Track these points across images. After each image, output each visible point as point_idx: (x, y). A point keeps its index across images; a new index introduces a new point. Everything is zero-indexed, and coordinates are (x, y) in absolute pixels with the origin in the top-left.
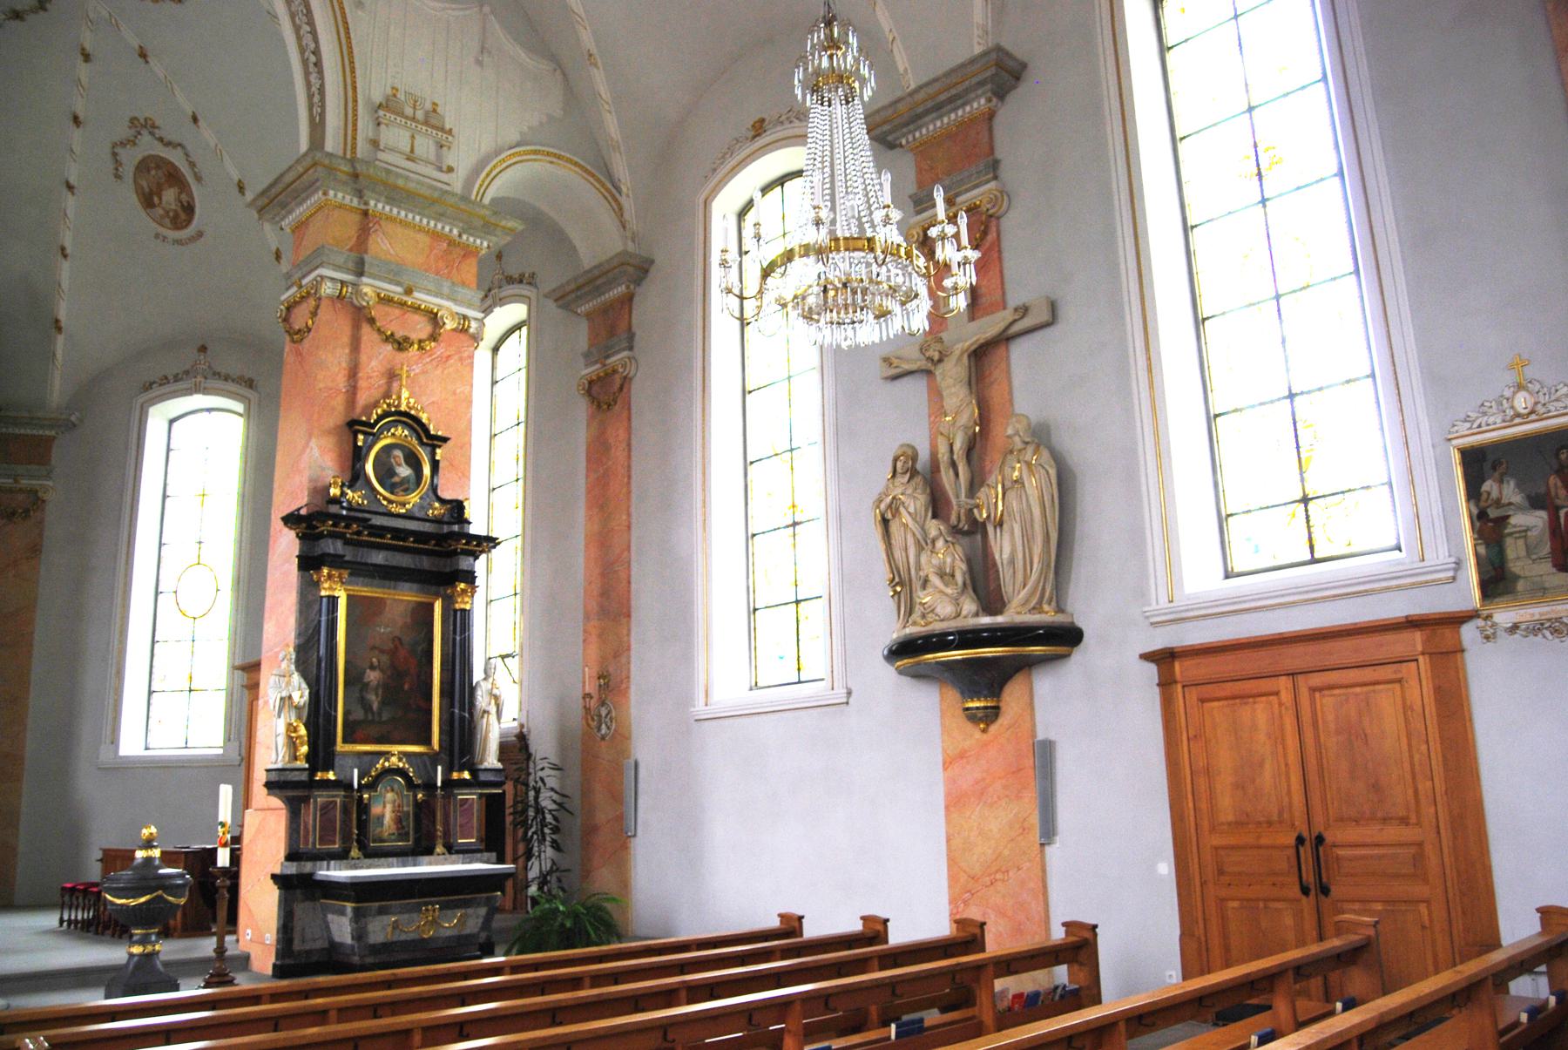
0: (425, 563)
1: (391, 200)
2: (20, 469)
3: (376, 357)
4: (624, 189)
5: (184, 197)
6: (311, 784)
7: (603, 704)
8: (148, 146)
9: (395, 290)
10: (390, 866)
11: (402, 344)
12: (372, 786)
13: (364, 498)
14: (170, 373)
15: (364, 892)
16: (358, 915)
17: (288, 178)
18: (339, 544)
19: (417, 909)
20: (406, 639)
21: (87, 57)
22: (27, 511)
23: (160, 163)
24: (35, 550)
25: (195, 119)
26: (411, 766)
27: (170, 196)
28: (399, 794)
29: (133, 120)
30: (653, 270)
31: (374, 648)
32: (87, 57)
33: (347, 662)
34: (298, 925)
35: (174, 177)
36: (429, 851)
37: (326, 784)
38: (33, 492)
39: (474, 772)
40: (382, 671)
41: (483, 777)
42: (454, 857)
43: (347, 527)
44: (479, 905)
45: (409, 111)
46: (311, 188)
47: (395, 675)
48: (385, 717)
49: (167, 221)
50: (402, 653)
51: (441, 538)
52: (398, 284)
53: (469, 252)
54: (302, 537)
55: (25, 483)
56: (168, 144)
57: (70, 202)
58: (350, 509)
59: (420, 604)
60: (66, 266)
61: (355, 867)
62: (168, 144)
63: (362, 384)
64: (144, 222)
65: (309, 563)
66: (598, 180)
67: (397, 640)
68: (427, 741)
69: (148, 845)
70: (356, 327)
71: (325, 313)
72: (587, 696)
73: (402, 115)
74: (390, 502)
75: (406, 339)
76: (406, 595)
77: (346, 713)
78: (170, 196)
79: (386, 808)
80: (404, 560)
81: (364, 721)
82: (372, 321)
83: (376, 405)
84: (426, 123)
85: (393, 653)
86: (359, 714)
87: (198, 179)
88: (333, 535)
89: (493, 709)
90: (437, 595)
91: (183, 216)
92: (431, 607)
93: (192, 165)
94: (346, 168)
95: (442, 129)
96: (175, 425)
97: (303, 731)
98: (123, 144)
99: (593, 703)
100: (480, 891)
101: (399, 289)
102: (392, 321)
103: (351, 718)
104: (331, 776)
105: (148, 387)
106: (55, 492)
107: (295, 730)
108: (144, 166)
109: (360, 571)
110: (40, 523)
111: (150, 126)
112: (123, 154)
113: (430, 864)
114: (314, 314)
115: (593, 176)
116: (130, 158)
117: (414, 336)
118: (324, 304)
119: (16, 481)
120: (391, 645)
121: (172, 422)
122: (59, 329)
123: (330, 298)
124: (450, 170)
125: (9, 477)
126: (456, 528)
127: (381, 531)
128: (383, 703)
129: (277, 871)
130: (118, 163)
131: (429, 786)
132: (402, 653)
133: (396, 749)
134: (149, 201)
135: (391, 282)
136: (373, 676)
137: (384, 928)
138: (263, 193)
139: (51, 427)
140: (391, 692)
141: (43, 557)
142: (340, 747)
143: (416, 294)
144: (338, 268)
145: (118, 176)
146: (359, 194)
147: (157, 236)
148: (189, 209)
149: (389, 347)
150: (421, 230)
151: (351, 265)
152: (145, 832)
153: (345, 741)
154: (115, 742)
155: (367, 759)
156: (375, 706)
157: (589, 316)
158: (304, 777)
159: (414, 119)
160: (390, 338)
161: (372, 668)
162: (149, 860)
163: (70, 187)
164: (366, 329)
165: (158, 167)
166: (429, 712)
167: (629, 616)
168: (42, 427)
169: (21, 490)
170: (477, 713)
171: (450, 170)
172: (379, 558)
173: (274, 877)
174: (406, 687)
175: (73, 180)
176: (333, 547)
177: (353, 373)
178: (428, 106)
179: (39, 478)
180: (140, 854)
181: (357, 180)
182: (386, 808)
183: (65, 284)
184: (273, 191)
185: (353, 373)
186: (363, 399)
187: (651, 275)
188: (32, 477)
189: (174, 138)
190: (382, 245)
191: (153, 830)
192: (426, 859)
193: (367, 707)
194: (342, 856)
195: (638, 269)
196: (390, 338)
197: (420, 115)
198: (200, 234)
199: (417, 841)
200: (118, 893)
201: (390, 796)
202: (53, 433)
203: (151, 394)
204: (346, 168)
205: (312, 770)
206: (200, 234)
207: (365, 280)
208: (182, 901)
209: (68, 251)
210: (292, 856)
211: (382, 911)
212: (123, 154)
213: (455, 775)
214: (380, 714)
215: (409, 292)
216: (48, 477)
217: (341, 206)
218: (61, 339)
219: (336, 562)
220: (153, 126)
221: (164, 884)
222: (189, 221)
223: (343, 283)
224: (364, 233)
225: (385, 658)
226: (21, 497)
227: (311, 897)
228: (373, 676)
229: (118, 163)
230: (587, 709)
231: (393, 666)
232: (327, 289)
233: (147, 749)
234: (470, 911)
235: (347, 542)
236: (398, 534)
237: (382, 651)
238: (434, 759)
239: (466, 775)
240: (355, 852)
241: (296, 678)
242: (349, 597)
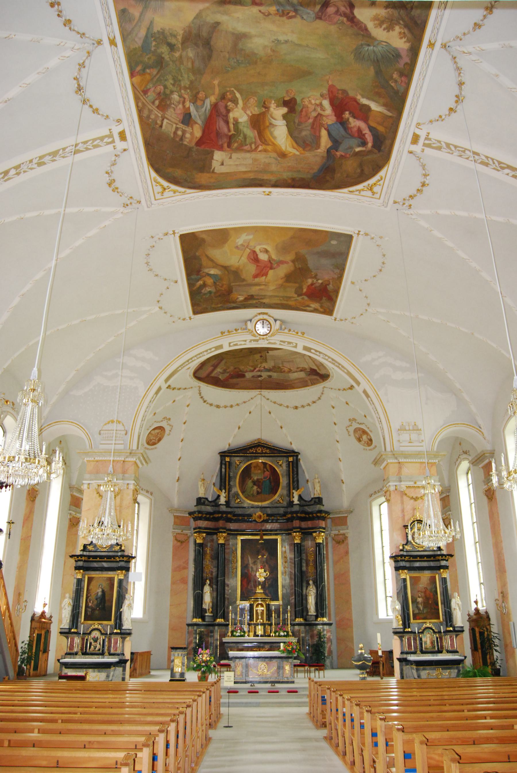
0: (432, 564)
1: (405, 458)
2: (339, 527)
3: (409, 504)
4: (482, 427)
5: (369, 437)
6: (404, 632)
7: (503, 602)
8: (355, 425)
9: (411, 484)
10: (429, 656)
11: (416, 499)
12: (422, 633)
13: (410, 547)
14: (377, 490)
15: (419, 664)
16: (417, 670)
17: (378, 458)
18: (404, 562)
19: (434, 669)
20: (429, 588)
21: (333, 407)
22: (343, 541)
23: (360, 429)
24: (347, 553)
25: (365, 416)
26: (434, 626)
27: (365, 437)
28: (431, 635)
29: (350, 420)
30: (495, 452)
31: (418, 591)
32: (333, 407)
33: (412, 597)
34: (405, 673)
35: (364, 432)
36: (441, 652)
37: (408, 632)
38: (344, 534)
39: (454, 627)
40: (423, 598)
41: (456, 629)
42: (449, 654)
43: (405, 558)
44: (454, 669)
45: (407, 428)
46: (384, 460)
47: (426, 599)
48: (425, 612)
49: (366, 445)
50: (428, 592)
51: (434, 556)
52: (412, 481)
53: (433, 464)
54: (395, 561)
55: (342, 532)
56: (361, 424)
57: (338, 445)
58: (407, 551)
59: (431, 577)
60: (341, 464)
61: (418, 656)
62: (361, 424)
63: (406, 514)
64: (359, 446)
65: (397, 569)
66: (473, 427)
67: (426, 588)
68: (439, 618)
69: (361, 649)
70: (402, 497)
71: (392, 496)
72: (496, 600)
73: (406, 430)
74: (418, 547)
75: (416, 497)
76: (426, 575)
77: (413, 611)
78: (365, 437)
79: (427, 639)
80: (425, 564)
81: (417, 614)
82: (406, 494)
83: (410, 519)
84: (413, 430)
85: (425, 592)
86: (417, 611)
87: (371, 431)
88: (401, 561)
89: (458, 608)
90: (437, 573)
91: (370, 442)
92: (435, 577)
93: (368, 428)
94: (390, 453)
95: (418, 430)
96: (381, 506)
97: (400, 617)
98: (348, 427)
99: (500, 602)
100: (455, 665)
101: (413, 483)
102: (412, 493)
103: (415, 612)
104: (410, 630)
105: (371, 496)
106: (350, 532)
107: (398, 617)
108: (355, 431)
109: (411, 569)
110: (347, 544)
111: (354, 420)
112: (349, 429)
113: (441, 656)
114: (390, 496)
115: (470, 426)
116: (351, 429)
117: (419, 496)
118: (392, 493)
119: (339, 532)
120: (424, 590)
121: (380, 505)
122: (343, 483)
123: (394, 491)
124: (422, 441)
125: (337, 530)
126: (439, 553)
127: (416, 556)
128: (424, 607)
129: (398, 657)
130: (349, 432)
131: (440, 632)
132: (428, 592)
133: (428, 621)
134: (359, 440)
135: (410, 481)
136: (420, 600)
137: (425, 674)
138: (374, 461)
139: (346, 513)
140: (426, 604)
141: (350, 554)
142: (412, 620)
143: (417, 483)
144: (394, 481)
145: (349, 435)
146: (396, 458)
147: (364, 449)
148: (371, 440)
149: (412, 501)
150: (416, 462)
151: (398, 480)
152: (360, 646)
153: (414, 619)
154: (377, 614)
155: (421, 624)
156: (421, 609)
157: (482, 468)
158: (402, 630)
159: (409, 430)
160: (412, 498)
161: (419, 597)
162: (362, 653)
163: (338, 442)
164: (405, 497)
165: (359, 430)
166: (438, 609)
167: (505, 572)
168: (343, 514)
169: (341, 534)
170: (452, 609)
171: (422, 441)
172: (417, 564)
173: (397, 659)
174: (430, 602)
175: (338, 440)
176: (402, 564)
177: (403, 511)
178: (413, 424)
179: (345, 530)
180: (360, 651)
181: (394, 455)
182: (427, 639)
183: (342, 469)
184: (376, 461)
185: (403, 511)
186: (406, 518)
187: (495, 454)
188: (343, 530)
189: (362, 422)
190: (406, 471)
191: (362, 645)
192: (440, 654)
193: (419, 609)
194: (415, 653)
195: (492, 454)
196: (412, 498)
197: (411, 428)
198: (376, 447)
199: (438, 648)
200: (355, 661)
201: (428, 635)
202: (346, 515)
203: (372, 498)
204: (390, 453)
205: (405, 627)
206: (376, 447)
207: (402, 483)
208: (370, 664)
209: (341, 459)
210: (402, 653)
211: (424, 669)
212: (349, 429)
213: (448, 629)
214: (423, 611)
215: (415, 483)
216: (347, 529)
217: (392, 463)
218: (344, 486)
219: (404, 568)
220: (355, 420)
221: (365, 659)
222: (372, 443)
223: (396, 486)
224: (400, 468)
225: (423, 594)
226: (341, 536)
227: (407, 665)
228: (420, 600)
229: (349, 432)
230: (497, 604)
231: (426, 596)
232: (392, 488)
233: (387, 616)
234: (452, 671)
235: (407, 561)
236: (421, 556)
237: (422, 592)
238: (441, 624)
239: (451, 629)
240: (418, 652)
241: (397, 602)
242: (410, 577)
